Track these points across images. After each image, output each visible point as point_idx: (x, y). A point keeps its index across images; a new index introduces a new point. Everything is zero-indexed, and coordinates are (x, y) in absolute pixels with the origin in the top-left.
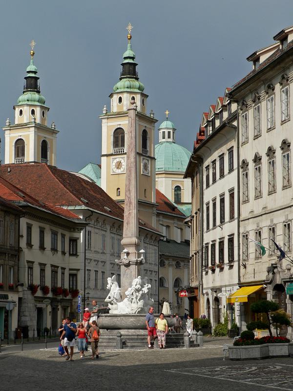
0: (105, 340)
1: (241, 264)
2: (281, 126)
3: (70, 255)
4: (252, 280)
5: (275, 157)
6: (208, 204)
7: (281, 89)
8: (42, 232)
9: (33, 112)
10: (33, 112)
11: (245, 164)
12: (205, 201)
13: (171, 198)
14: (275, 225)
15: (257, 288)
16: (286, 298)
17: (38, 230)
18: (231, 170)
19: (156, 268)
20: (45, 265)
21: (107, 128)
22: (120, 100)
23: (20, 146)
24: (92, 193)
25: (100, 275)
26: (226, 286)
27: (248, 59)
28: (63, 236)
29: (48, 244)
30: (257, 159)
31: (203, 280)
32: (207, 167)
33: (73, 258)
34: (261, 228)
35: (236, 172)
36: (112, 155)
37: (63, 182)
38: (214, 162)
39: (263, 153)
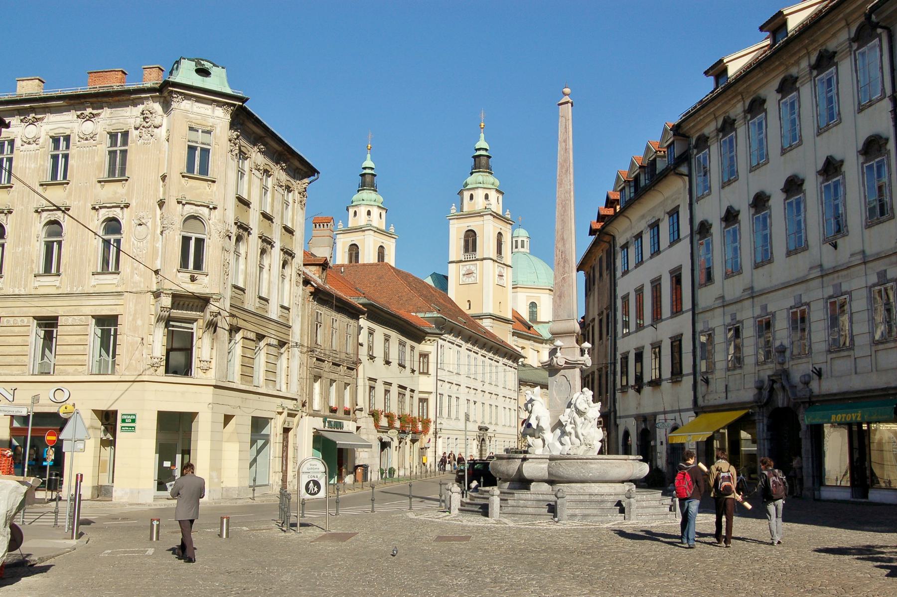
0: (530, 503)
1: (699, 378)
2: (783, 158)
3: (420, 373)
4: (723, 401)
5: (770, 208)
6: (626, 298)
7: (779, 101)
8: (387, 339)
9: (369, 213)
10: (369, 213)
11: (704, 229)
12: (620, 293)
13: (526, 316)
14: (773, 314)
15: (740, 413)
16: (800, 430)
17: (382, 338)
18: (675, 239)
19: (515, 395)
20: (390, 384)
21: (456, 230)
22: (472, 197)
23: (354, 250)
24: (441, 301)
25: (454, 400)
26: (665, 413)
27: (706, 73)
28: (413, 348)
29: (394, 357)
30: (731, 217)
31: (617, 405)
32: (625, 246)
33: (423, 378)
34: (738, 322)
35: (685, 245)
36: (461, 261)
37: (409, 284)
38: (639, 236)
39: (742, 203)
